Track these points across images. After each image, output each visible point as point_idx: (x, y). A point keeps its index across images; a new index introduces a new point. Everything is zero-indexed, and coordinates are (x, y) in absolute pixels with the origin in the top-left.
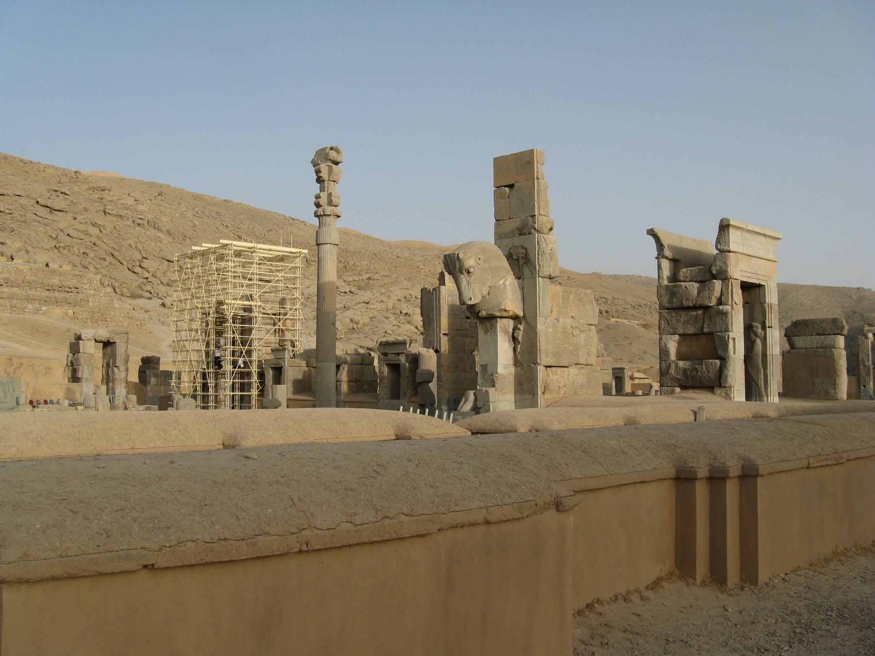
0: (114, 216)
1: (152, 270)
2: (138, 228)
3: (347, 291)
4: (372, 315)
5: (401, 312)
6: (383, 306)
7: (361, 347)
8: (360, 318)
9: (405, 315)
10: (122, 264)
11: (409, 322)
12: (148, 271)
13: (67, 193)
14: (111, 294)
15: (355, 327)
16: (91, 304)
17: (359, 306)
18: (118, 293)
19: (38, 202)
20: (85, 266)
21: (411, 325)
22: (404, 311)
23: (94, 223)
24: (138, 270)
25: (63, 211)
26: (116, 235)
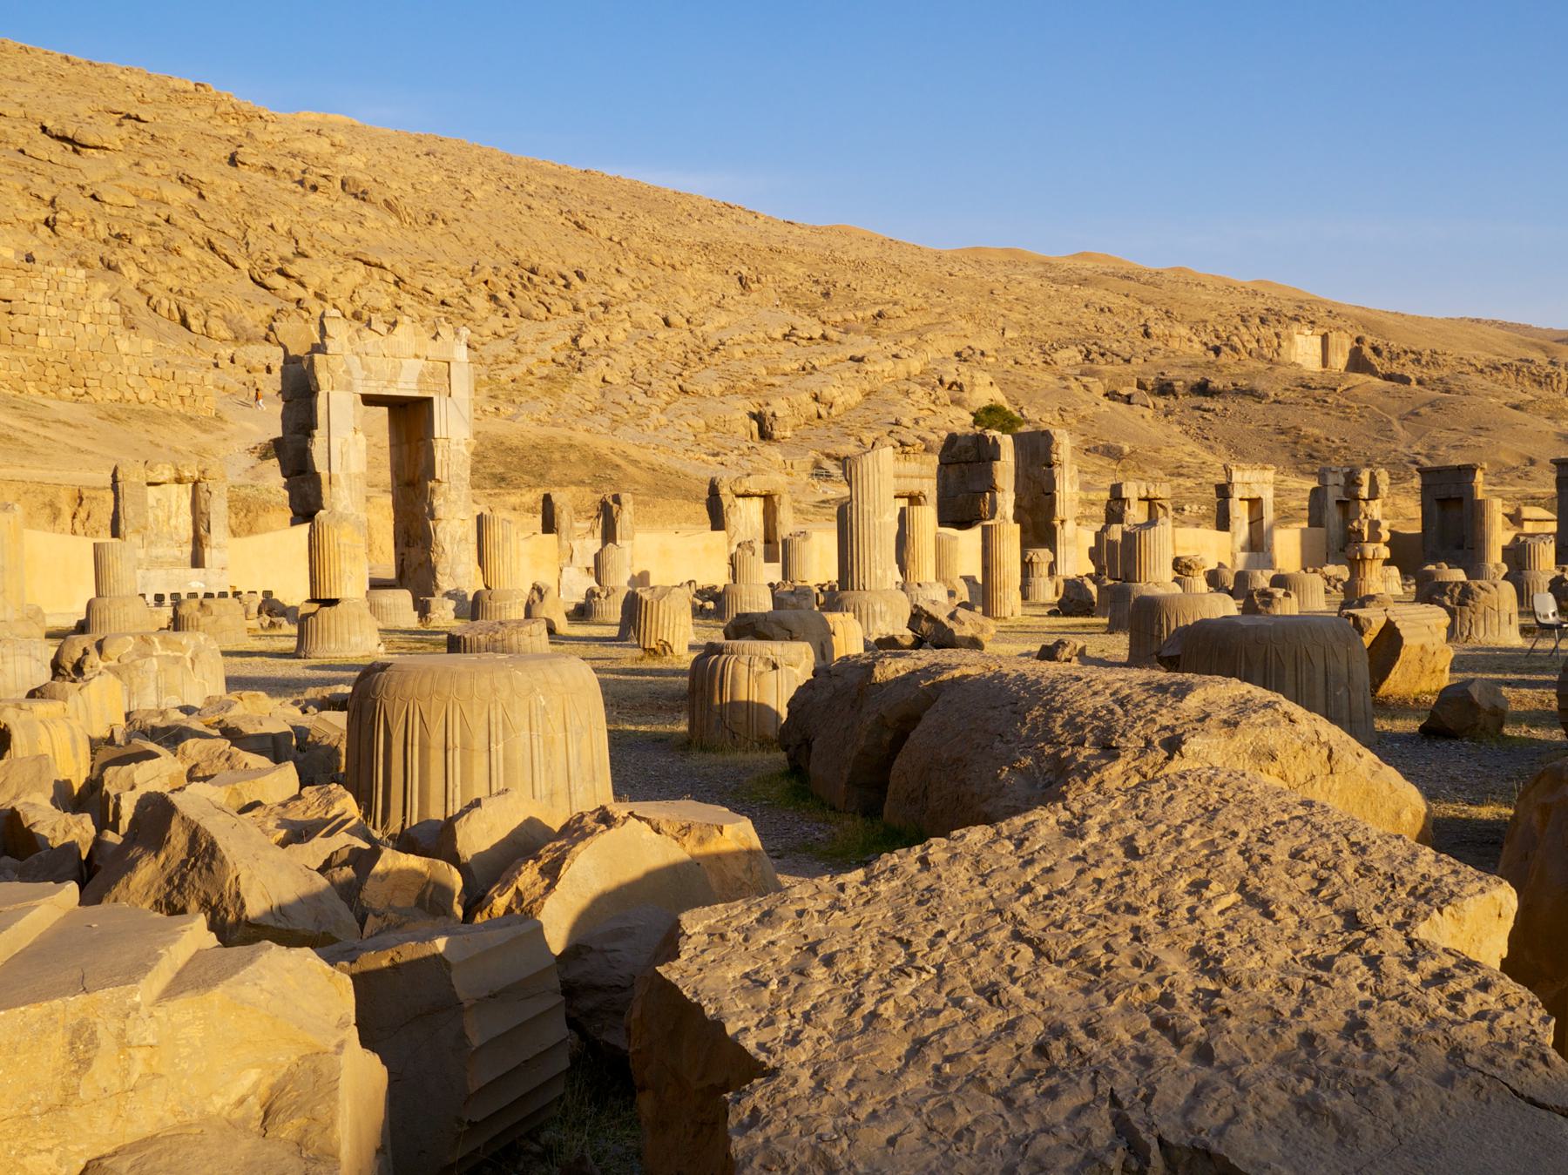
0: (256, 171)
1: (313, 283)
2: (312, 197)
3: (817, 335)
4: (868, 388)
5: (941, 381)
6: (901, 368)
7: (828, 456)
8: (835, 392)
9: (950, 388)
10: (235, 267)
11: (957, 402)
12: (303, 285)
13: (142, 117)
14: (112, 317)
15: (823, 413)
16: (43, 342)
17: (839, 366)
18: (193, 328)
19: (44, 129)
20: (113, 264)
21: (964, 407)
22: (948, 379)
23: (186, 178)
24: (278, 281)
25: (106, 149)
26: (243, 205)
